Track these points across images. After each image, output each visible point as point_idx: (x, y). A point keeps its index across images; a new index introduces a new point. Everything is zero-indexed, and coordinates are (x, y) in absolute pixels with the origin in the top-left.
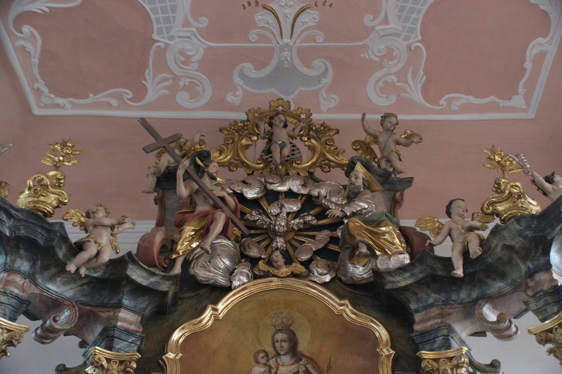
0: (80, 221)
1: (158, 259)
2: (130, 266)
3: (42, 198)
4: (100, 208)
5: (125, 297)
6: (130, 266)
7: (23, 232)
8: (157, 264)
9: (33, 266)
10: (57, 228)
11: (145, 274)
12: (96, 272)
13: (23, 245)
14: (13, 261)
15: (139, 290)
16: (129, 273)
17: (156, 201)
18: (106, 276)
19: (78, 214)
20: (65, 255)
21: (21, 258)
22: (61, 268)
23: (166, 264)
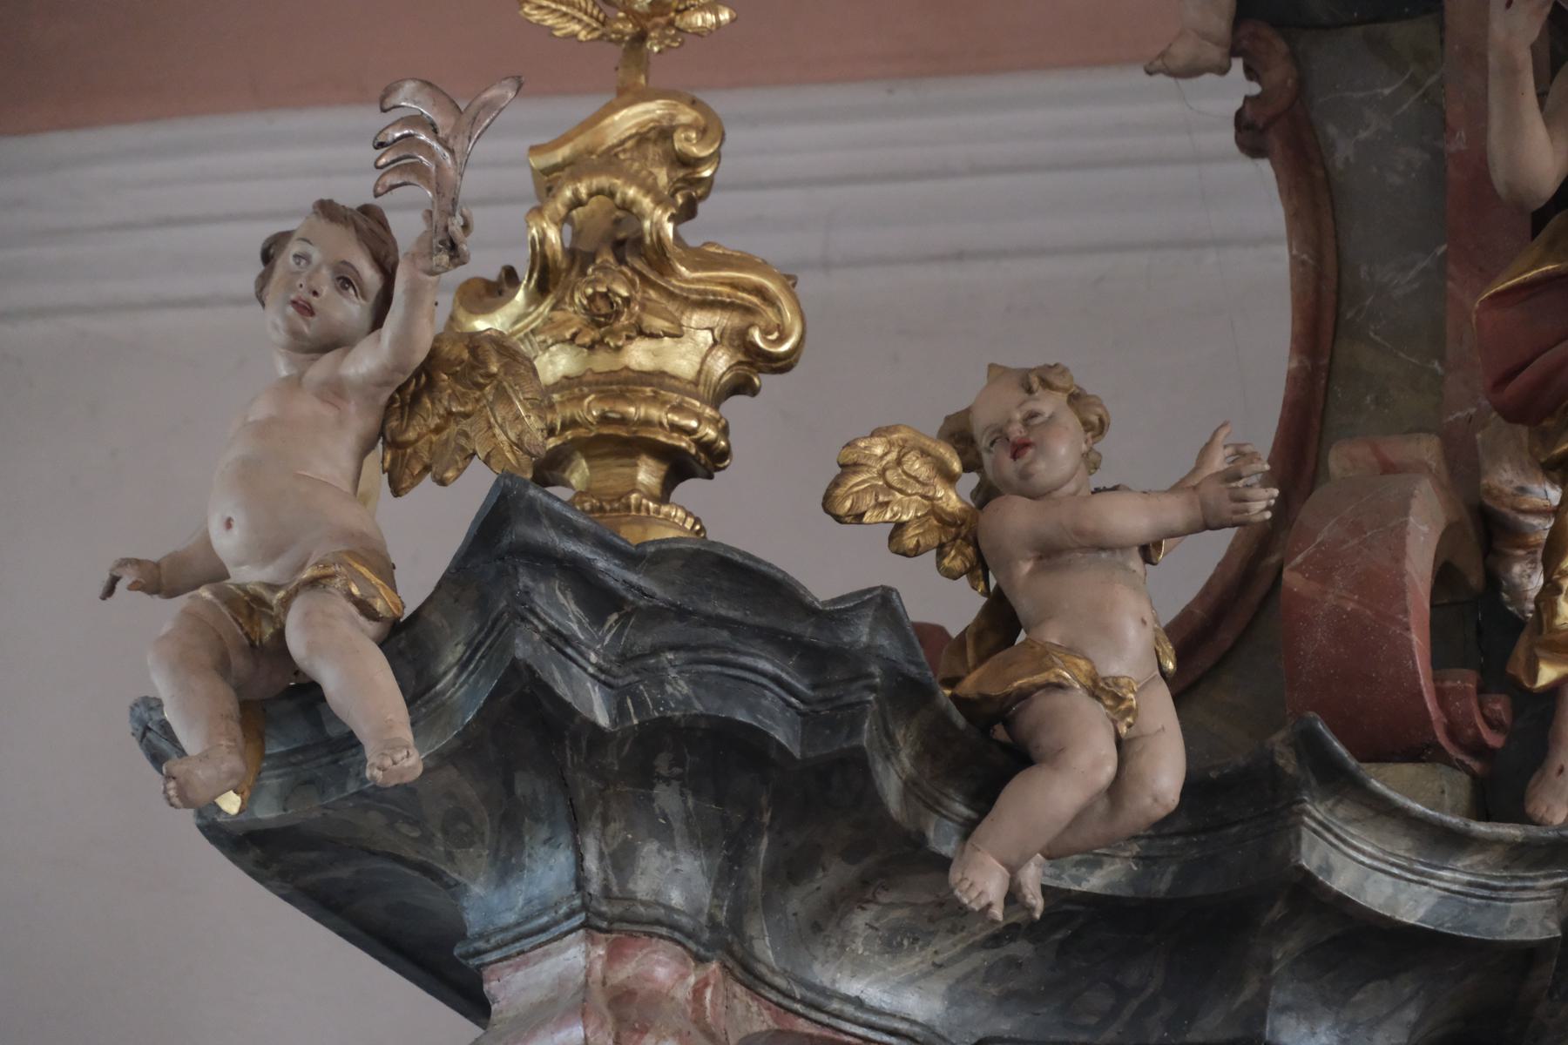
0: (935, 511)
1: (1441, 695)
2: (1316, 810)
3: (639, 355)
4: (1047, 404)
5: (1279, 996)
6: (1316, 810)
7: (679, 689)
8: (1443, 740)
9: (728, 875)
10: (863, 633)
11: (1402, 847)
12: (1095, 863)
13: (678, 761)
14: (621, 860)
15: (1363, 948)
16: (1312, 855)
17: (1251, 133)
18: (1162, 885)
19: (916, 466)
20: (910, 787)
21: (664, 835)
22: (900, 866)
23: (1493, 724)
